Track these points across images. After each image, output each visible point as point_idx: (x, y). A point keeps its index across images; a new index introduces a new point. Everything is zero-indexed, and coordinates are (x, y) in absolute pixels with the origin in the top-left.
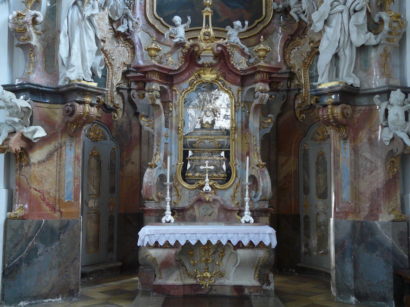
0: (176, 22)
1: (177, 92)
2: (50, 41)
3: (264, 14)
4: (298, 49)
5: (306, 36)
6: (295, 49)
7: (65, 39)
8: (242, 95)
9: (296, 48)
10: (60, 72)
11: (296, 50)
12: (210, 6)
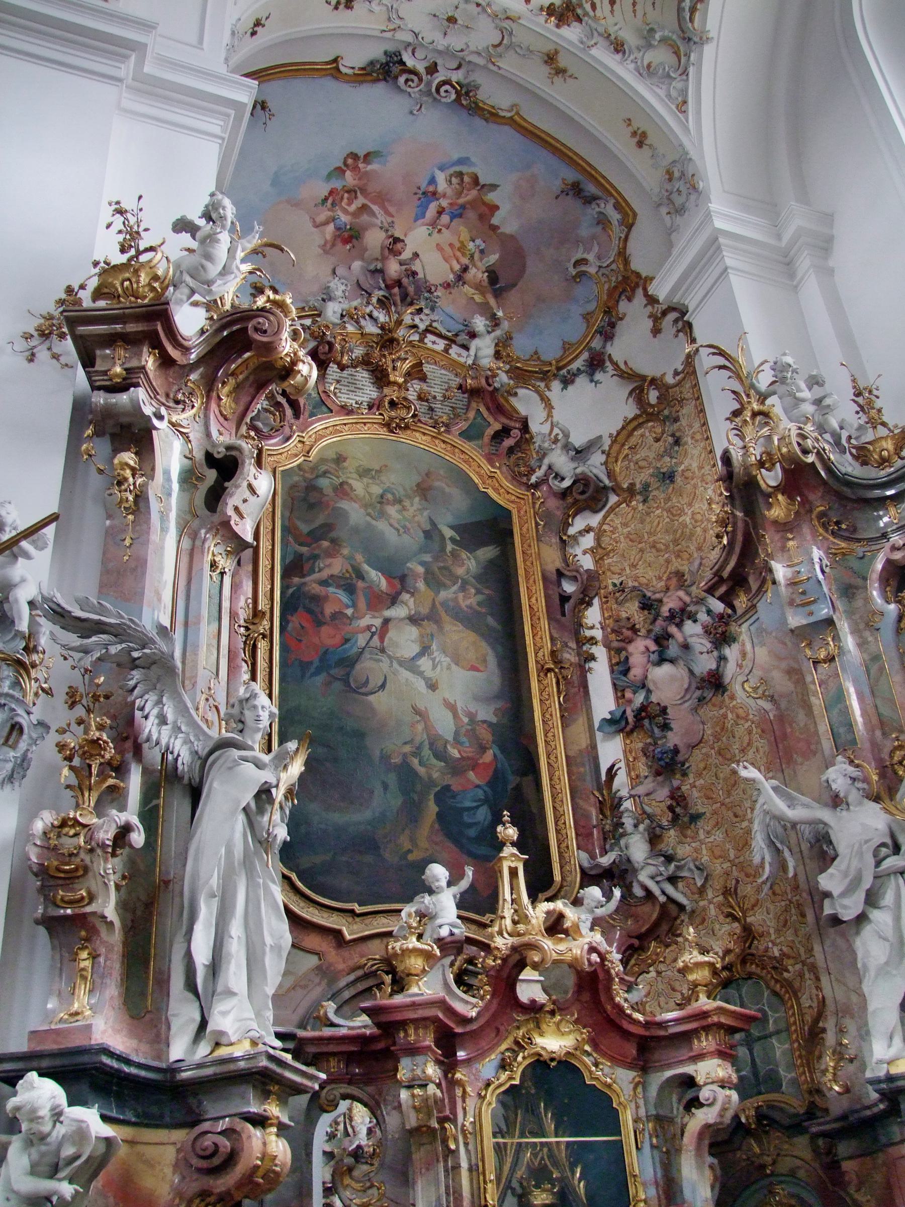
0: (438, 881)
1: (469, 1089)
2: (139, 913)
3: (557, 877)
4: (659, 973)
5: (680, 939)
6: (648, 973)
7: (208, 906)
8: (645, 1098)
9: (651, 969)
10: (174, 1015)
11: (653, 974)
12: (513, 844)
